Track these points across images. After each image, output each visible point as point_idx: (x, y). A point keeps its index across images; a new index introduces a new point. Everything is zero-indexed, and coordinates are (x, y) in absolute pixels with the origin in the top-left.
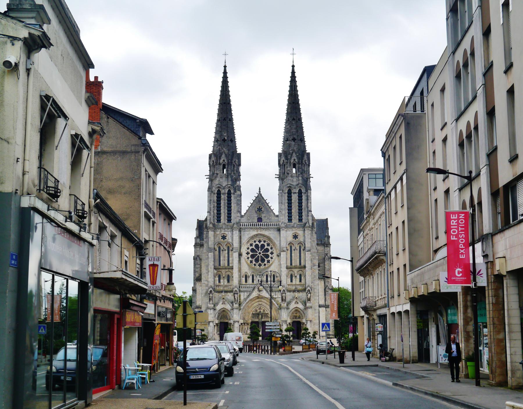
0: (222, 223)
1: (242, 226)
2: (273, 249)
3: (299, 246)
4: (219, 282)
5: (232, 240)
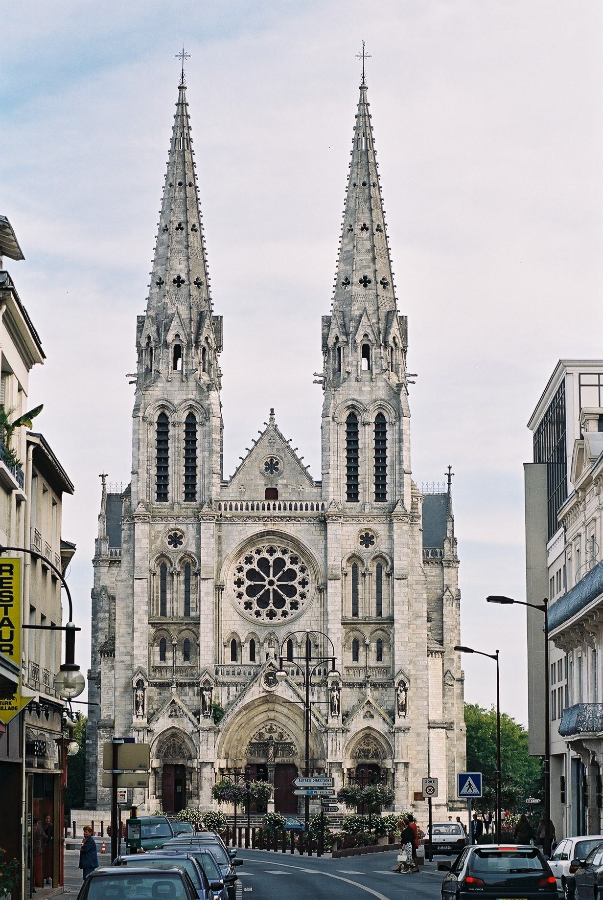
0: (170, 502)
1: (226, 509)
2: (308, 571)
3: (375, 564)
5: (198, 547)
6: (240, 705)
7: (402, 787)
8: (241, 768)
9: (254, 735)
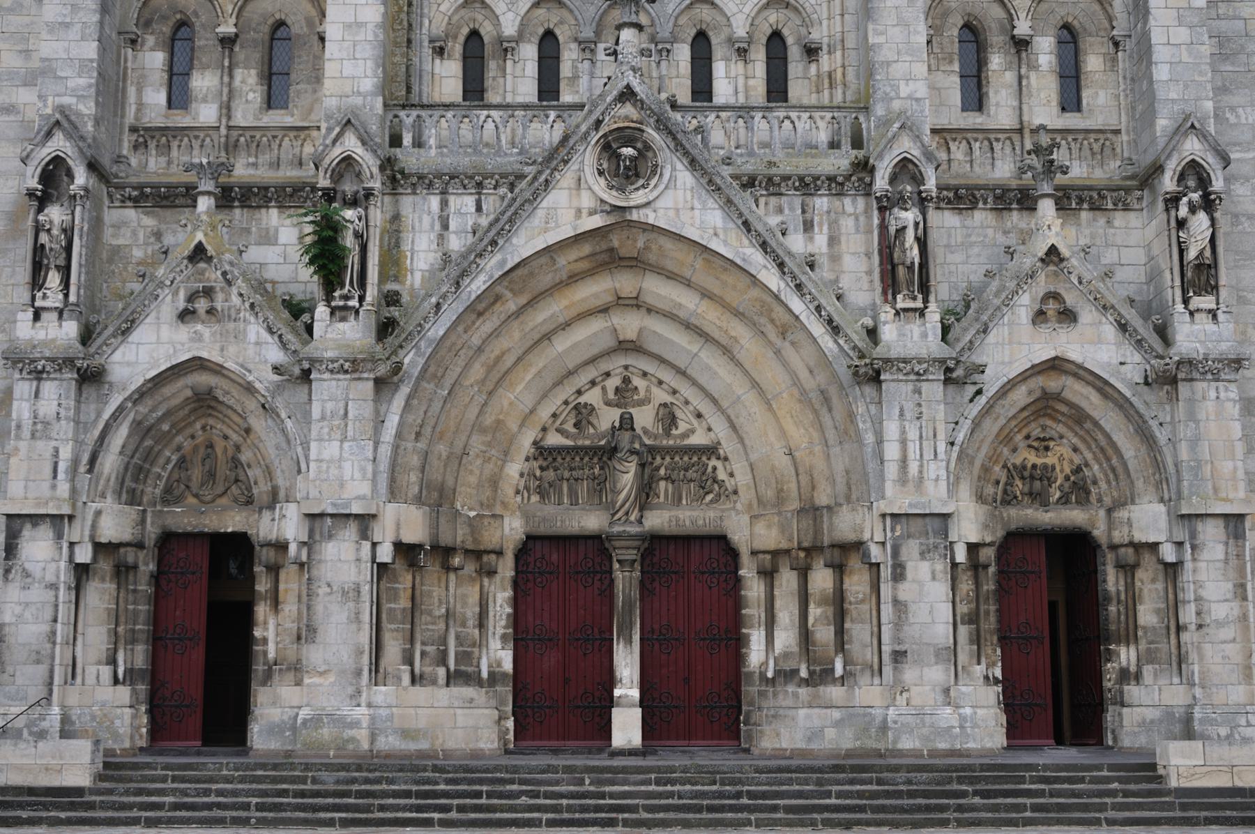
4: (178, 97)
6: (492, 266)
7: (1220, 624)
8: (499, 553)
9: (554, 415)
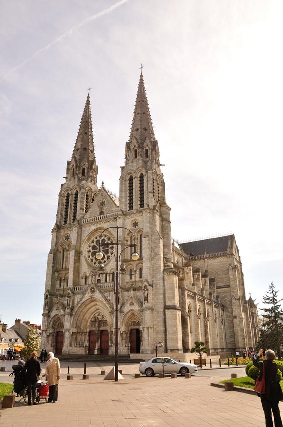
3: (139, 235)
